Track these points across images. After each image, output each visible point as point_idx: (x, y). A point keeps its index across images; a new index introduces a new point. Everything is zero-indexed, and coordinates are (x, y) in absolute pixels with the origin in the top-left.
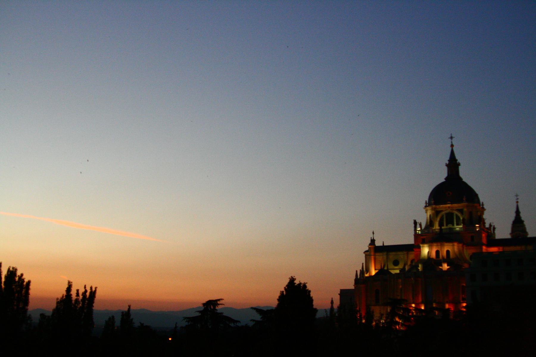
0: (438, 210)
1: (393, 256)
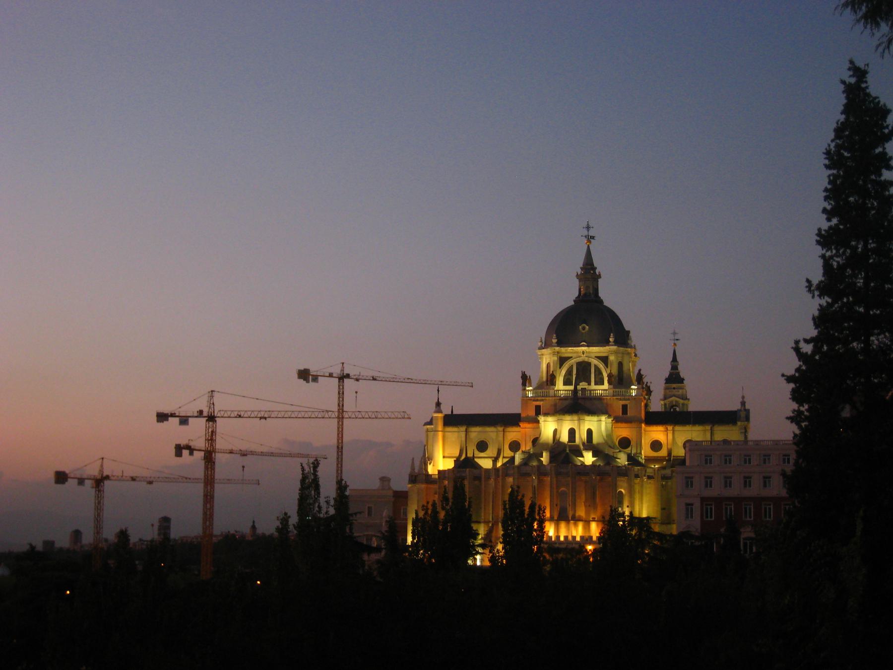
0: (564, 355)
1: (476, 433)
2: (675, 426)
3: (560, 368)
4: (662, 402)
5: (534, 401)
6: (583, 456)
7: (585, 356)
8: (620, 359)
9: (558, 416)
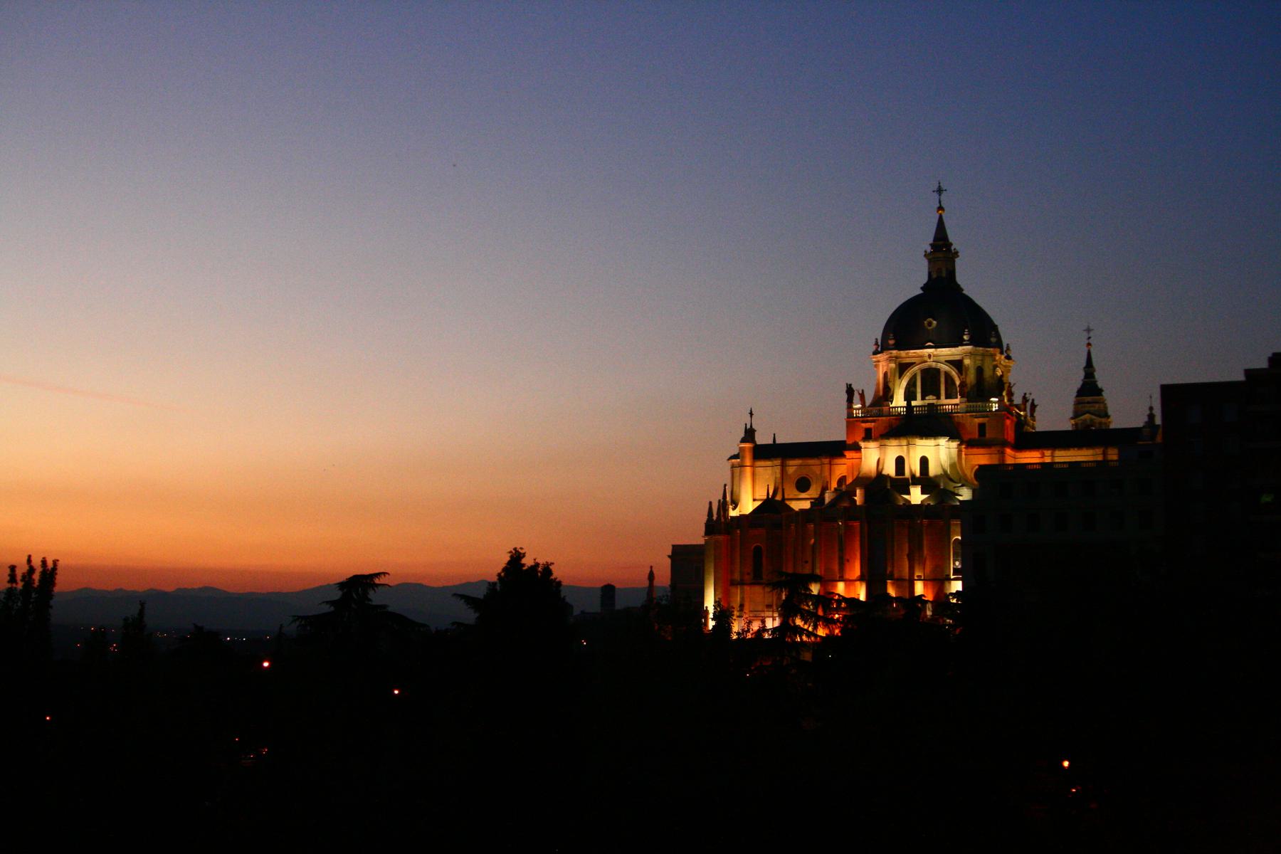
1: (793, 466)
2: (1055, 450)
3: (900, 378)
4: (1073, 422)
5: (863, 422)
6: (909, 493)
7: (932, 360)
8: (979, 363)
9: (880, 441)
